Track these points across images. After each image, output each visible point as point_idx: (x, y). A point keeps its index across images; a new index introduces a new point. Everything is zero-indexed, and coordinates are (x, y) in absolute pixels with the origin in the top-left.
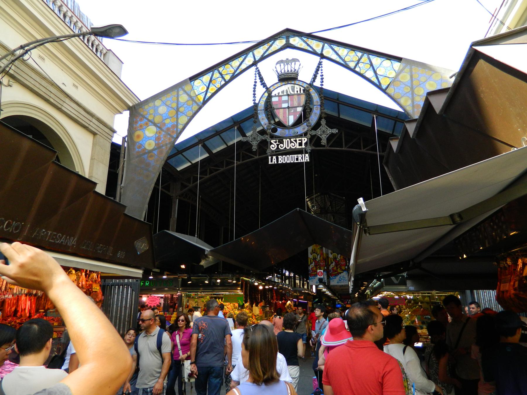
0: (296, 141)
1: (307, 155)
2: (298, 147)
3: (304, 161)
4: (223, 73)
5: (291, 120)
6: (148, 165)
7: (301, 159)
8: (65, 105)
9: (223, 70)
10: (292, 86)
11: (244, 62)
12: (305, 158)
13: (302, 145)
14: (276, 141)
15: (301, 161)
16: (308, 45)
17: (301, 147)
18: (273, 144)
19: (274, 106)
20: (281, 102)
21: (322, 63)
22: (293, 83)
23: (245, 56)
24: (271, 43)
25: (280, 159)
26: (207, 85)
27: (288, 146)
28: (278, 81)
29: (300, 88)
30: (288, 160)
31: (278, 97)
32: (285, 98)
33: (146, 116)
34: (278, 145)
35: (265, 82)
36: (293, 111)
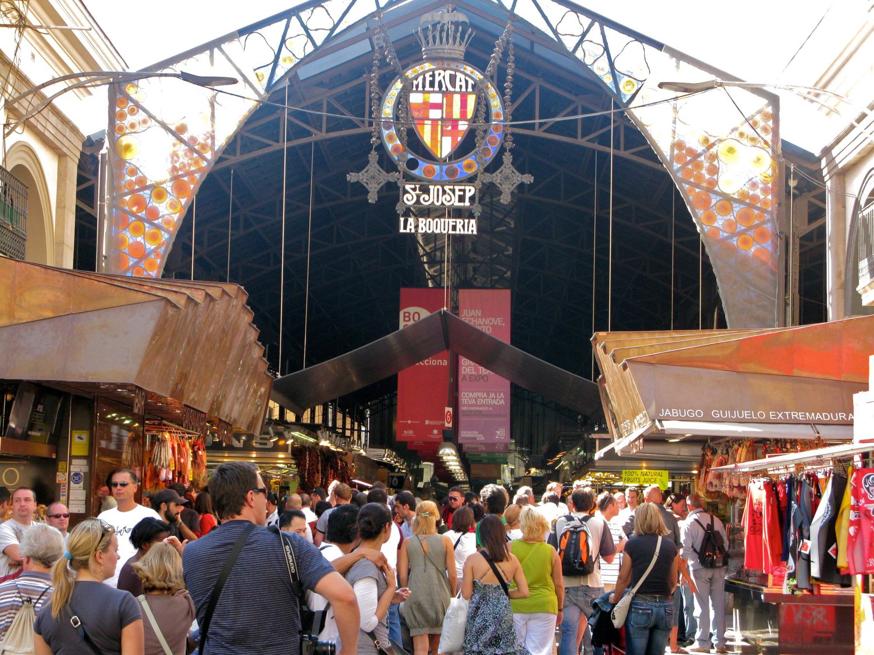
0: (453, 191)
1: (473, 222)
2: (457, 204)
3: (466, 232)
4: (310, 26)
5: (446, 147)
6: (153, 214)
10: (450, 75)
12: (470, 227)
13: (464, 202)
14: (416, 188)
15: (462, 232)
17: (462, 204)
18: (409, 193)
19: (416, 114)
22: (455, 67)
25: (421, 225)
27: (438, 201)
29: (467, 82)
31: (422, 94)
34: (418, 196)
36: (450, 128)
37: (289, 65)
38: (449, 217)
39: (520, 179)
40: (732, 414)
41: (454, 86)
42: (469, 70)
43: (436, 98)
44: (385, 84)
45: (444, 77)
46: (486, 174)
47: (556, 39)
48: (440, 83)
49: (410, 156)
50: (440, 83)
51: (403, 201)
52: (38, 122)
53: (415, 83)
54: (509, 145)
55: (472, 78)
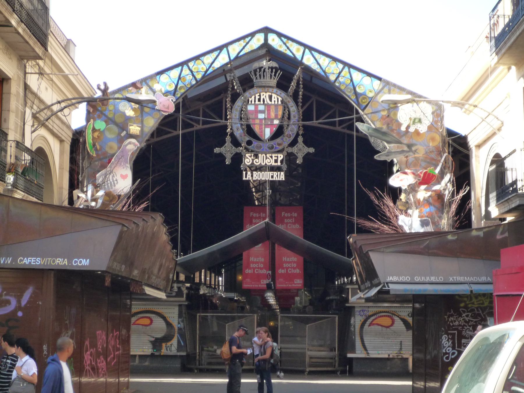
0: (271, 157)
1: (282, 173)
2: (274, 164)
3: (279, 179)
4: (193, 70)
5: (268, 133)
7: (276, 177)
8: (55, 126)
9: (193, 66)
12: (280, 176)
14: (251, 155)
15: (277, 179)
16: (288, 48)
18: (247, 158)
19: (251, 116)
20: (257, 111)
23: (218, 51)
24: (247, 40)
25: (254, 175)
26: (176, 83)
29: (278, 99)
32: (261, 108)
33: (104, 112)
34: (253, 160)
37: (183, 91)
38: (268, 171)
39: (307, 150)
40: (426, 278)
41: (271, 101)
42: (279, 92)
43: (261, 108)
44: (233, 101)
45: (266, 96)
46: (289, 148)
47: (325, 76)
51: (245, 163)
52: (49, 123)
53: (250, 99)
54: (301, 132)
55: (281, 97)
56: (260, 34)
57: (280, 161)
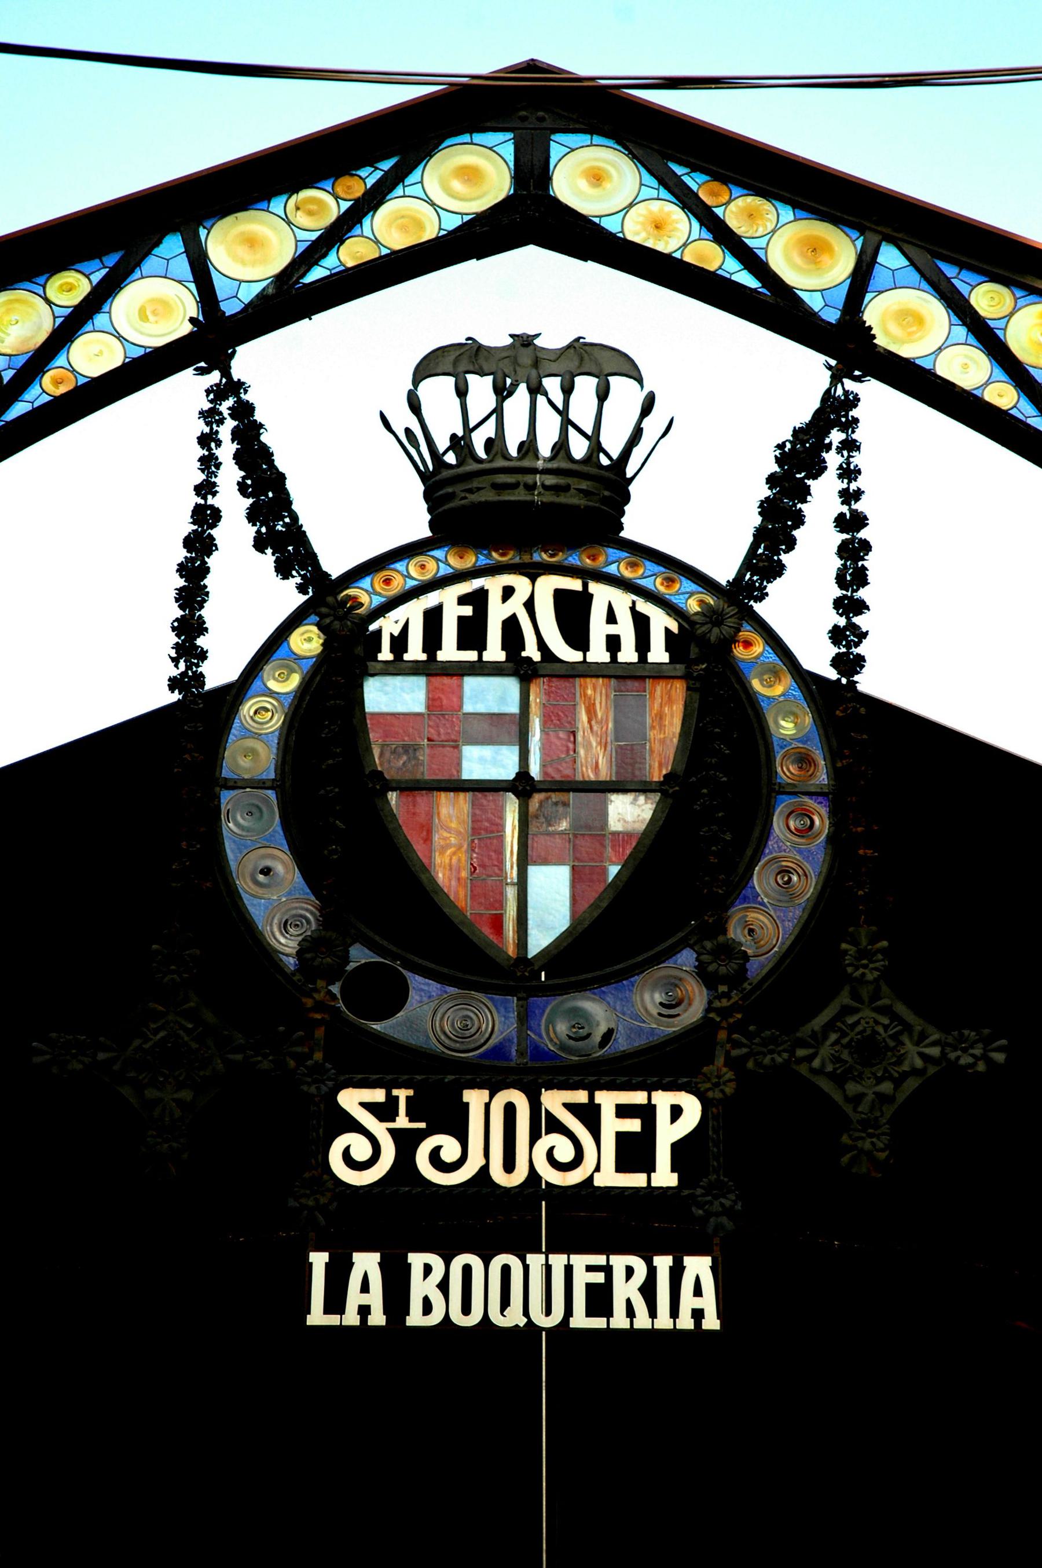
0: (590, 1116)
2: (609, 1178)
3: (664, 1322)
11: (100, 319)
13: (649, 1166)
15: (642, 1321)
17: (638, 1180)
21: (854, 413)
22: (574, 559)
24: (370, 176)
25: (420, 1288)
27: (509, 1165)
28: (427, 533)
29: (641, 623)
30: (505, 1302)
34: (407, 1142)
35: (307, 522)
45: (529, 605)
48: (511, 626)
49: (359, 955)
50: (511, 626)
53: (388, 625)
56: (478, 138)
57: (676, 1147)
